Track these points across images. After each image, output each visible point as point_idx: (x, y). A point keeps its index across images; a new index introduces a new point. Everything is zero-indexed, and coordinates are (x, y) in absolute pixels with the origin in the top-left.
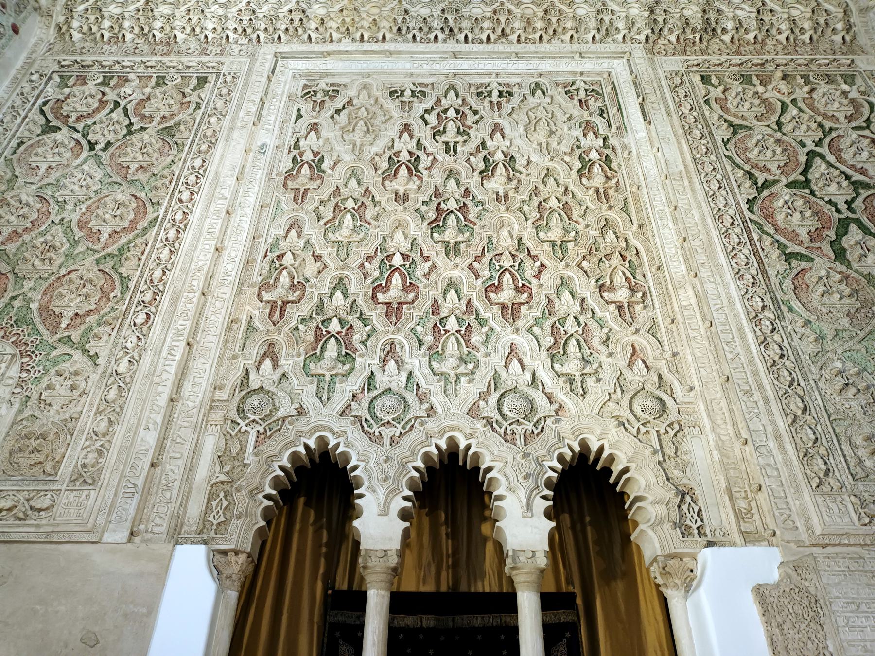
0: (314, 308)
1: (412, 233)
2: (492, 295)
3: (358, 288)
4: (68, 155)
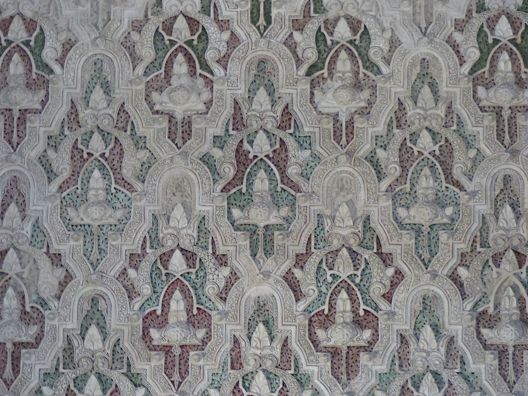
1: (198, 208)
2: (320, 333)
3: (123, 318)
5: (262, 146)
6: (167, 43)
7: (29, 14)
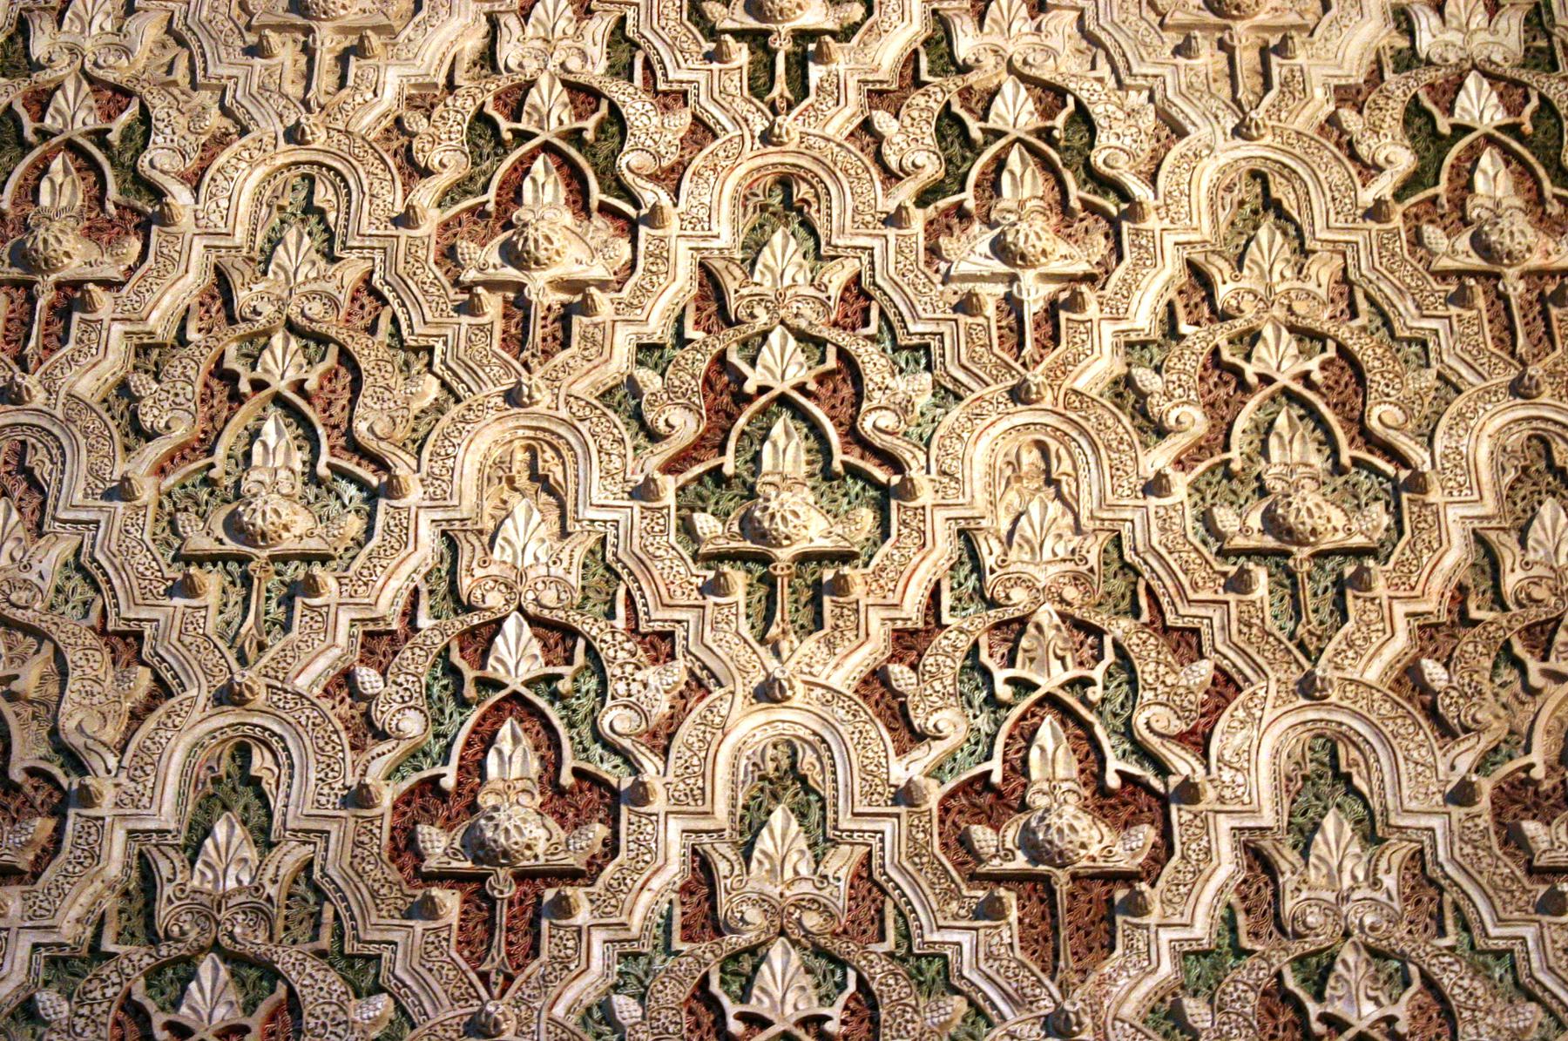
0: (110, 903)
6: (508, 136)
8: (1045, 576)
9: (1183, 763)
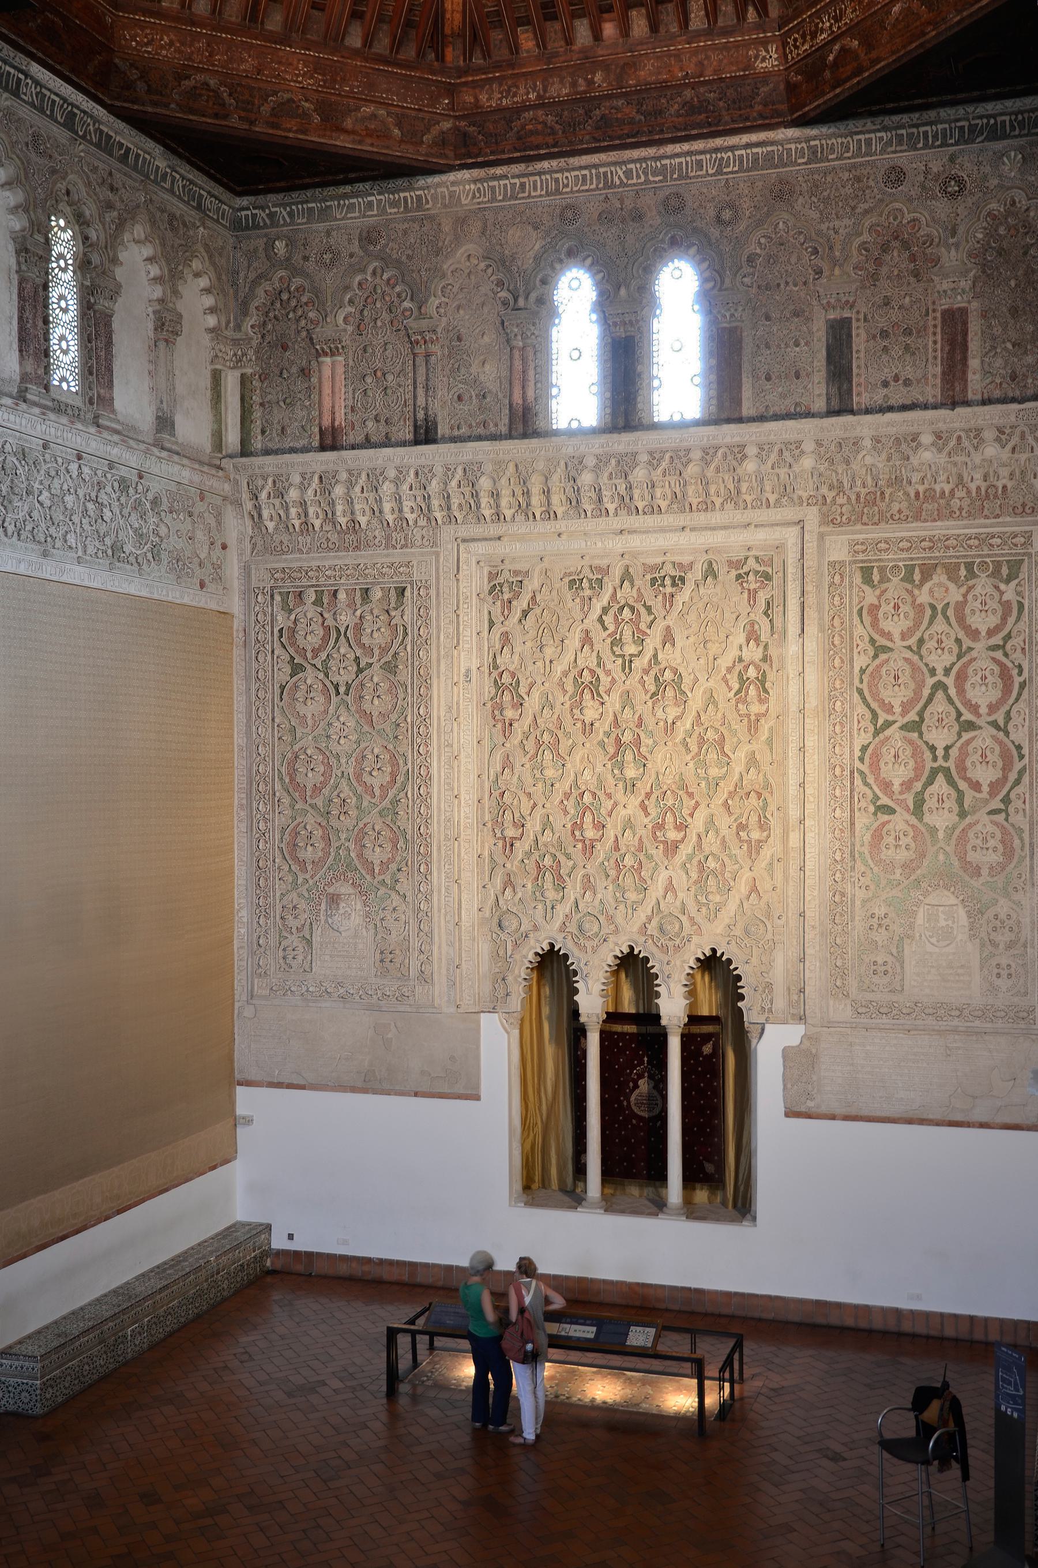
4: (322, 699)
5: (627, 737)
7: (511, 669)
8: (669, 782)
9: (689, 820)
